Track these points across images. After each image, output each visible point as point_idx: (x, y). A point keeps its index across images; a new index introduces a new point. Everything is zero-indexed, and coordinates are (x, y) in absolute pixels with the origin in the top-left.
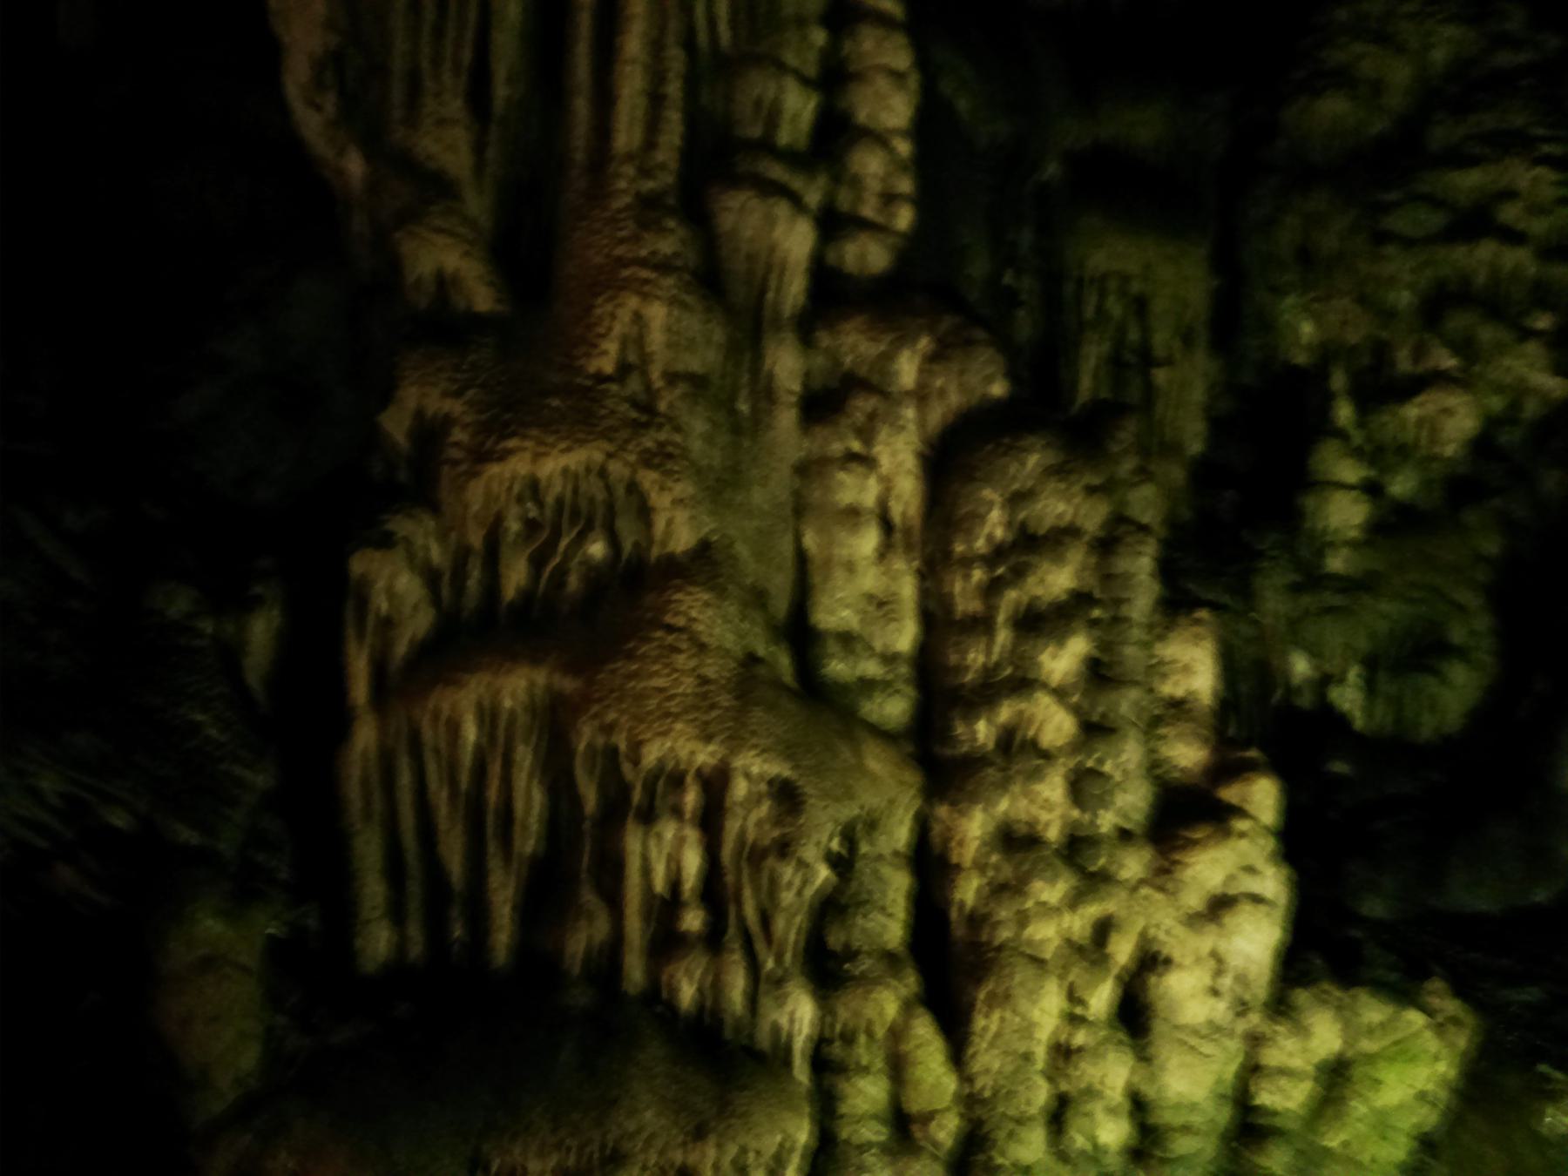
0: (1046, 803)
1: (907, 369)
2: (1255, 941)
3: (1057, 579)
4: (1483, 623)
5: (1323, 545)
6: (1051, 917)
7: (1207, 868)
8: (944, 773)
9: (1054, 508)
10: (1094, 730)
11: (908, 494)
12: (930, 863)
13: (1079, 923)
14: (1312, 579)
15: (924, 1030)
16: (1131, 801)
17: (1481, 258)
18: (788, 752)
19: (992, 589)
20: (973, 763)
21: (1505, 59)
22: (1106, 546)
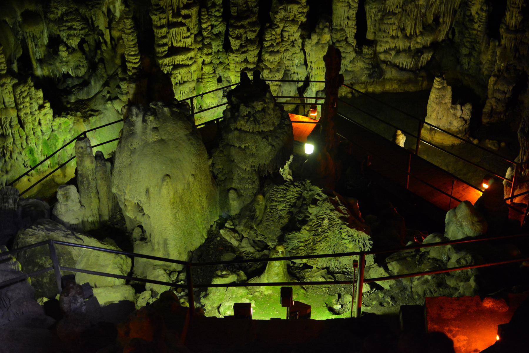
0: (28, 111)
1: (9, 81)
2: (50, 116)
3: (25, 94)
4: (85, 62)
5: (63, 57)
6: (30, 119)
7: (44, 111)
8: (19, 110)
9: (23, 90)
10: (31, 104)
11: (11, 89)
12: (19, 117)
13: (33, 118)
14: (62, 62)
15: (21, 129)
16: (37, 107)
17: (72, 32)
18: (5, 114)
19: (20, 96)
20: (21, 109)
21: (71, 10)
22: (29, 89)
